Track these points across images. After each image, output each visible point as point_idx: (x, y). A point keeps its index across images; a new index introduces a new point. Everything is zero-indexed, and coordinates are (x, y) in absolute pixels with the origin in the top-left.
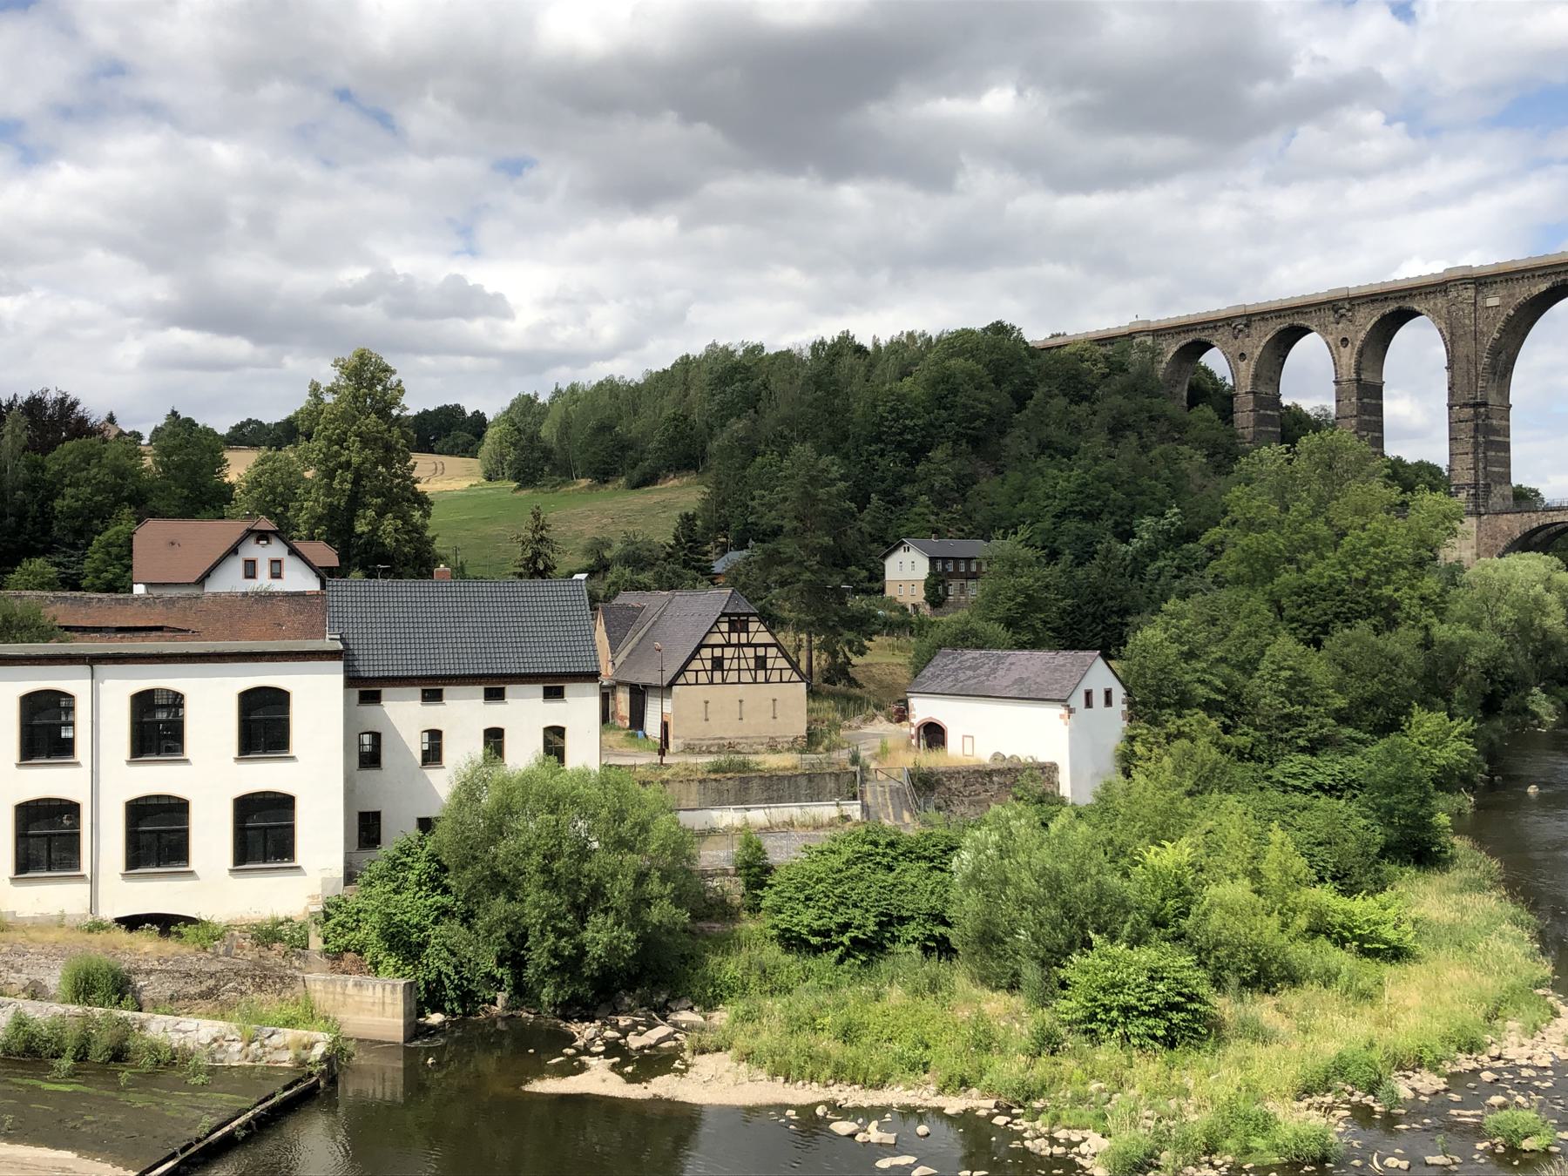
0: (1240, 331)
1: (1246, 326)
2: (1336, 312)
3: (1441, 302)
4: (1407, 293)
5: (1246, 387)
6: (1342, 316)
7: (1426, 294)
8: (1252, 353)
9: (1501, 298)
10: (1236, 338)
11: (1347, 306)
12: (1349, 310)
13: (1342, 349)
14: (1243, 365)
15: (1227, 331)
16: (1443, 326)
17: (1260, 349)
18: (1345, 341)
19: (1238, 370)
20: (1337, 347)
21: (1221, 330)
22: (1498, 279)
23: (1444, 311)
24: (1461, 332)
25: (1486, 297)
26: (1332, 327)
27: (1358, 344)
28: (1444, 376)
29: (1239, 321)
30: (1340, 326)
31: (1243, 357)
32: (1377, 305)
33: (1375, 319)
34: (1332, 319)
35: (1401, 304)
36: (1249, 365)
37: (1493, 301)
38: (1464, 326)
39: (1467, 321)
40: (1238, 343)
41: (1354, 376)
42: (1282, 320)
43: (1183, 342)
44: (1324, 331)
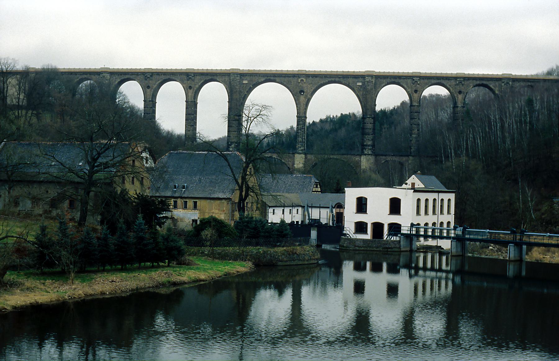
0: (148, 77)
1: (151, 76)
2: (188, 76)
3: (227, 78)
4: (215, 74)
5: (149, 98)
6: (191, 78)
7: (222, 75)
8: (153, 86)
9: (248, 81)
10: (146, 80)
11: (193, 75)
12: (193, 77)
13: (189, 90)
14: (148, 90)
15: (142, 77)
16: (227, 87)
17: (156, 85)
18: (190, 88)
19: (146, 92)
20: (187, 89)
21: (139, 76)
22: (248, 75)
23: (228, 82)
24: (235, 91)
25: (243, 80)
26: (185, 82)
27: (195, 89)
28: (227, 105)
29: (149, 74)
30: (189, 82)
31: (148, 87)
32: (204, 77)
33: (202, 81)
34: (186, 79)
35: (213, 77)
36: (151, 90)
37: (245, 82)
38: (236, 89)
39: (237, 87)
40: (146, 82)
41: (193, 100)
42: (166, 76)
43: (123, 78)
44: (182, 82)
